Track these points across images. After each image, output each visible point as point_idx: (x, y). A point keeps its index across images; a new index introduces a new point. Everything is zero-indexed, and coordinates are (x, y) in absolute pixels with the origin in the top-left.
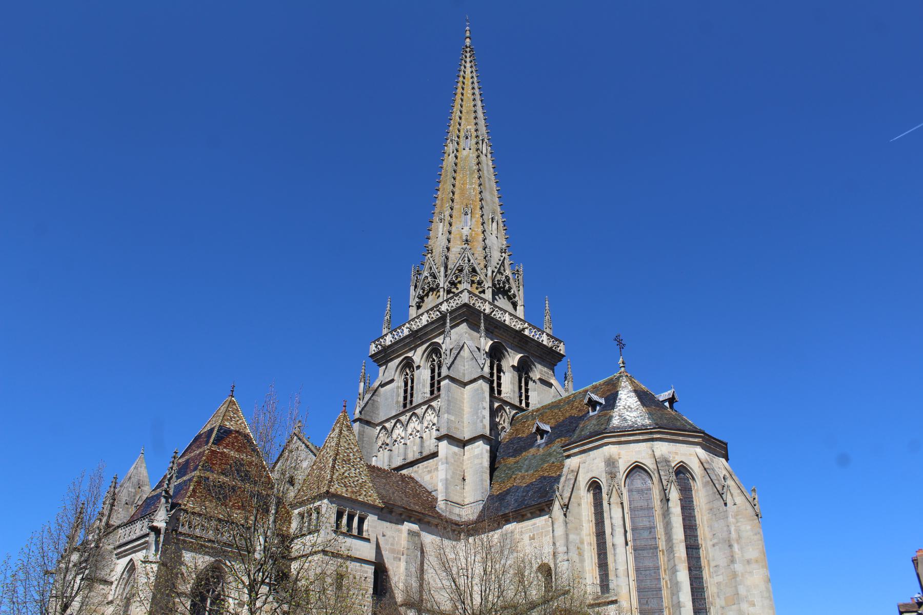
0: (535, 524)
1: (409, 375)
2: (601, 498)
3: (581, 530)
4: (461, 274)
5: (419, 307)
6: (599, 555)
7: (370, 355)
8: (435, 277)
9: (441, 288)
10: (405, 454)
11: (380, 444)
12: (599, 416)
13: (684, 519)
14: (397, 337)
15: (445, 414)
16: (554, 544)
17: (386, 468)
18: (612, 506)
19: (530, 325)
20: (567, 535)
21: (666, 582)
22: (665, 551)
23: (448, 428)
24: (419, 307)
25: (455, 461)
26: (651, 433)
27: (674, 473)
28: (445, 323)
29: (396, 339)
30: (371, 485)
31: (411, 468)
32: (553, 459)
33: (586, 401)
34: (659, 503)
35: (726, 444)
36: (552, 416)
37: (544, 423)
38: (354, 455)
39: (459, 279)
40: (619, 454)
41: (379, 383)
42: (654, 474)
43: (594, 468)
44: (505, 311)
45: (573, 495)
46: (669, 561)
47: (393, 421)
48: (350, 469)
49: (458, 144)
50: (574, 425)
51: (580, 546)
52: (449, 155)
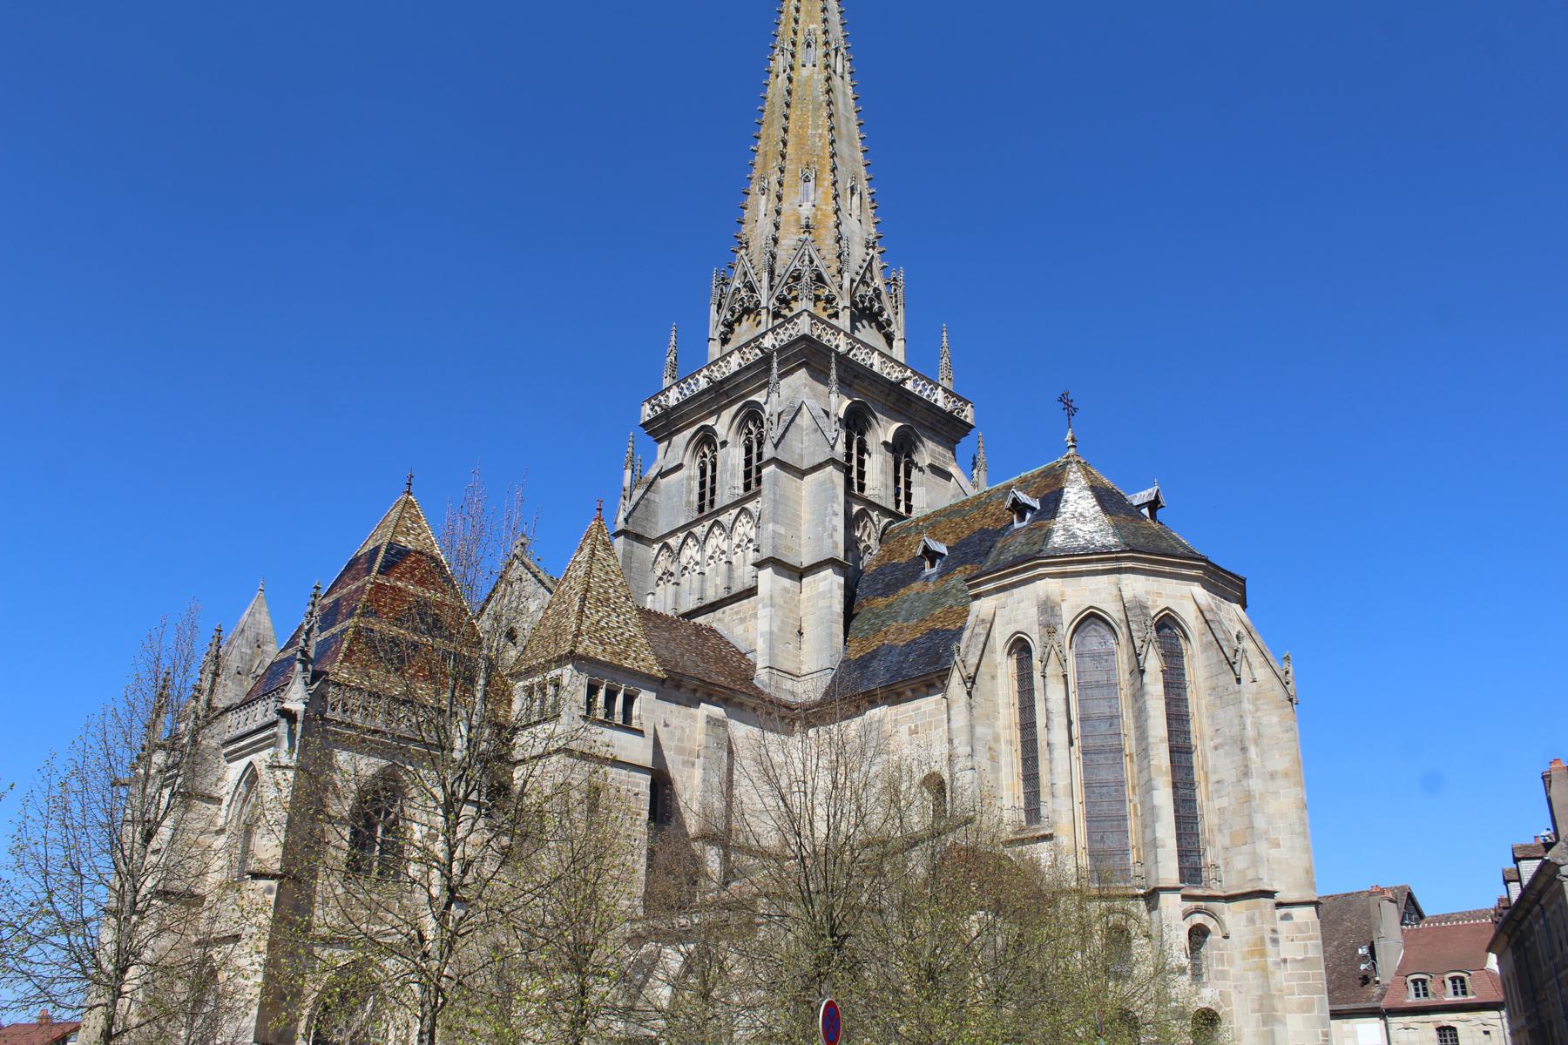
0: (918, 708)
1: (709, 457)
2: (1030, 667)
3: (996, 718)
5: (725, 341)
6: (1025, 760)
7: (642, 422)
8: (752, 290)
9: (764, 308)
10: (702, 590)
11: (659, 572)
12: (1030, 529)
13: (1167, 704)
16: (950, 741)
17: (670, 613)
18: (1048, 680)
19: (914, 373)
20: (972, 727)
21: (1135, 806)
22: (1135, 756)
23: (775, 547)
24: (725, 341)
25: (785, 602)
26: (1118, 559)
27: (1153, 628)
28: (769, 369)
29: (685, 395)
30: (644, 641)
31: (712, 614)
32: (951, 601)
33: (1008, 504)
34: (1127, 676)
35: (1244, 581)
36: (950, 527)
37: (937, 540)
38: (615, 591)
39: (794, 293)
40: (1062, 594)
42: (1120, 628)
43: (1020, 617)
44: (873, 349)
45: (984, 659)
46: (1140, 772)
47: (682, 535)
48: (610, 615)
49: (793, 56)
50: (988, 544)
51: (992, 745)
52: (777, 76)
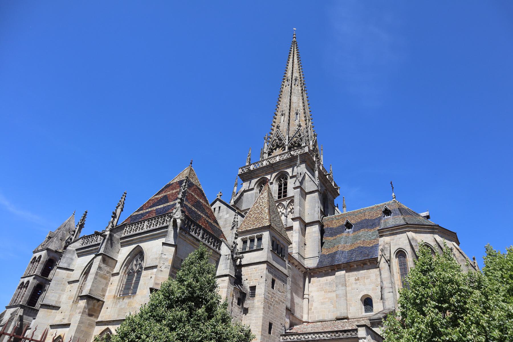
7: (239, 174)
15: (297, 206)
41: (243, 189)
43: (400, 243)
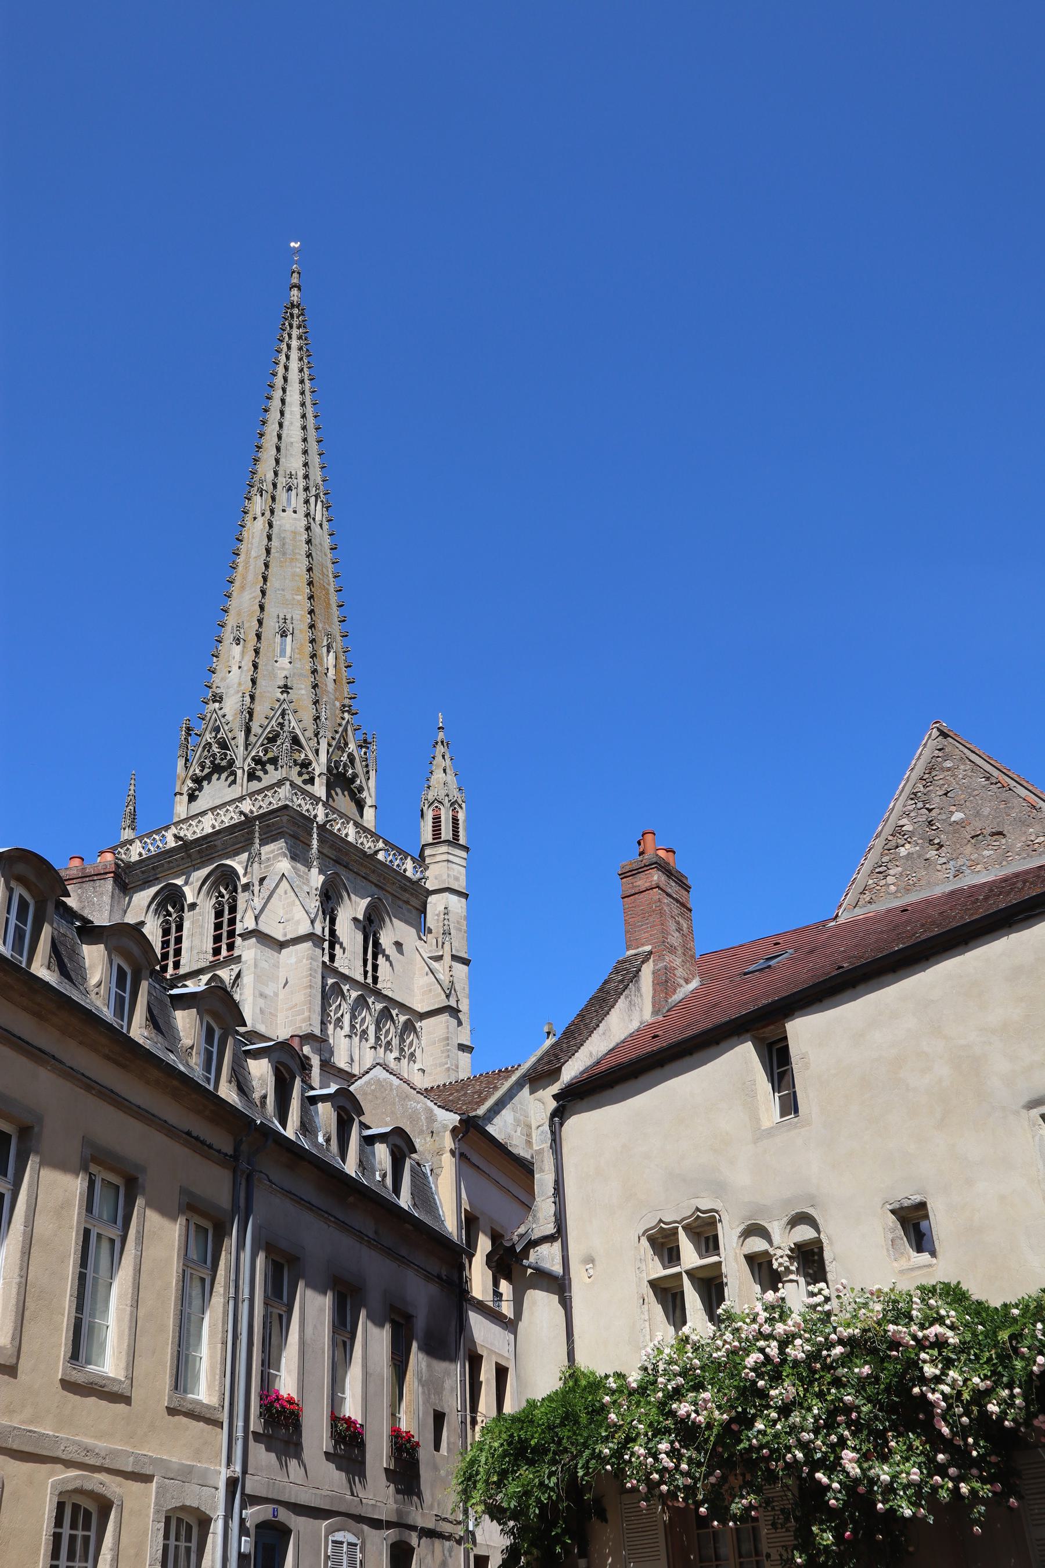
4: (274, 746)
5: (192, 798)
8: (223, 745)
14: (152, 849)
19: (386, 842)
24: (192, 798)
29: (149, 850)
39: (270, 755)
44: (348, 819)
49: (273, 499)
52: (255, 518)
